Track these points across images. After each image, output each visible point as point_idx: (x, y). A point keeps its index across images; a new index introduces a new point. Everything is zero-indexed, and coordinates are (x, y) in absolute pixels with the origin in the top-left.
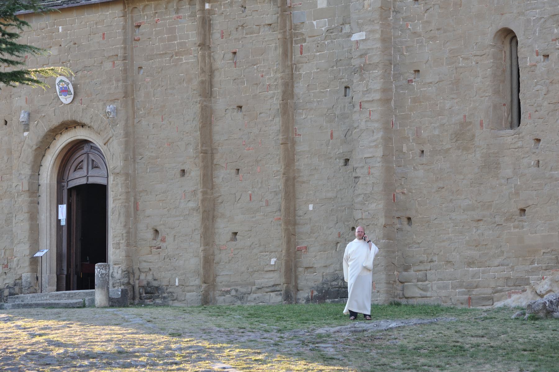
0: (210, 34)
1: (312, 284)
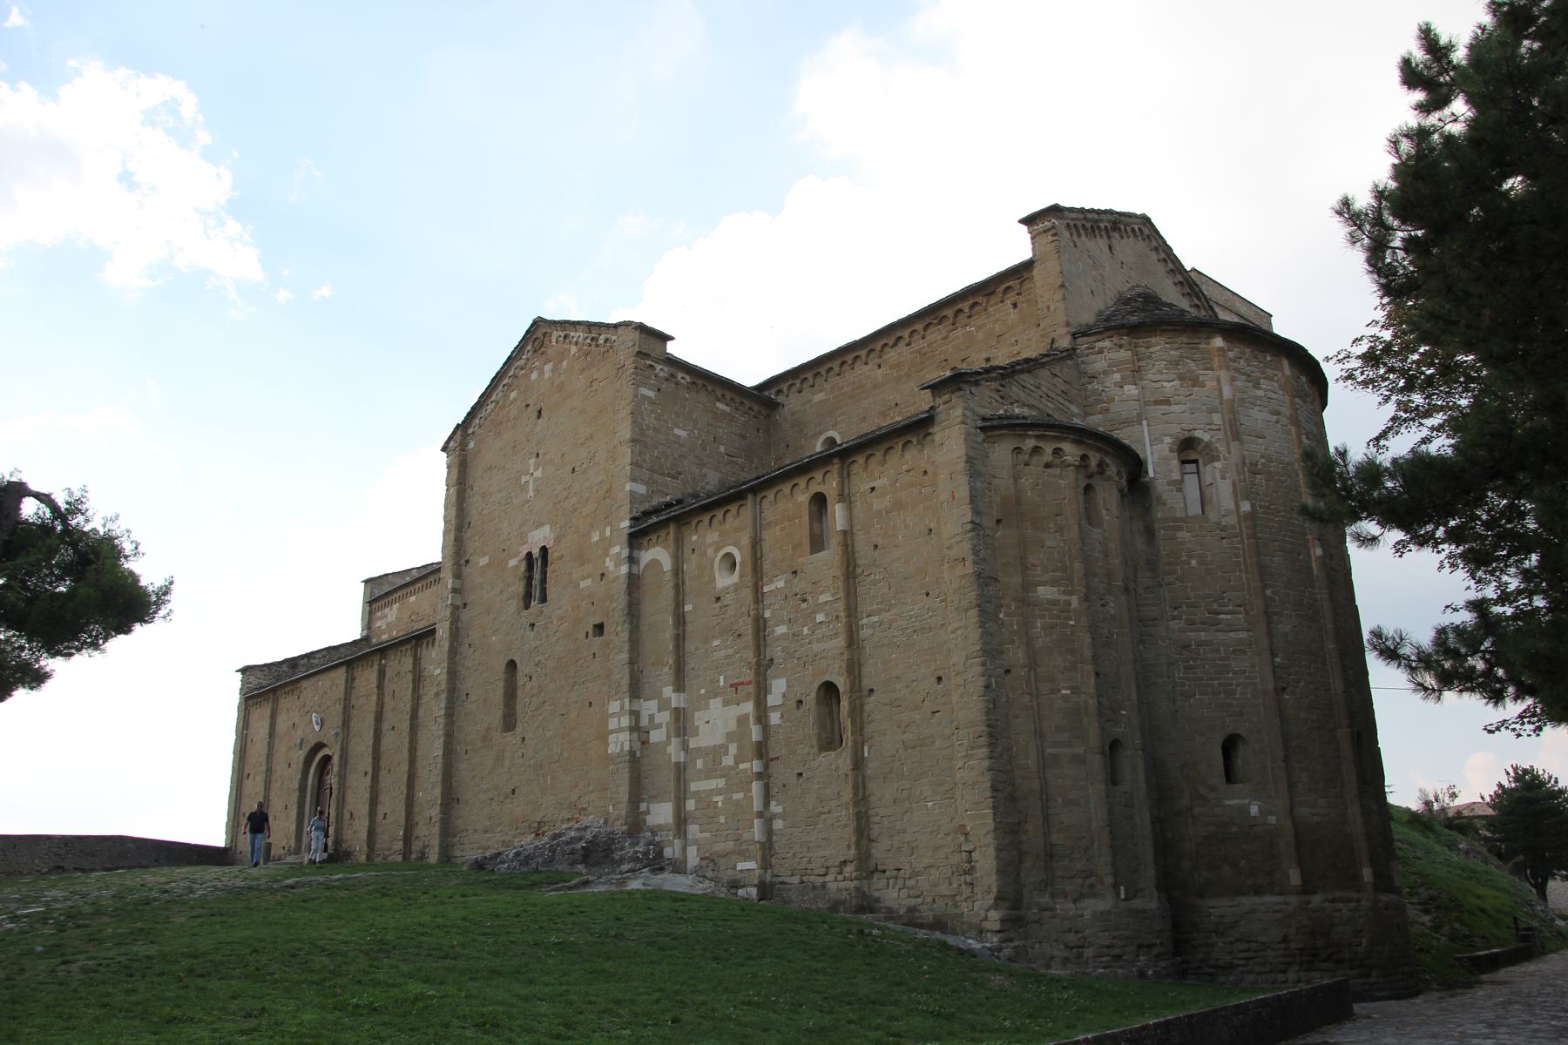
0: (384, 679)
1: (418, 848)
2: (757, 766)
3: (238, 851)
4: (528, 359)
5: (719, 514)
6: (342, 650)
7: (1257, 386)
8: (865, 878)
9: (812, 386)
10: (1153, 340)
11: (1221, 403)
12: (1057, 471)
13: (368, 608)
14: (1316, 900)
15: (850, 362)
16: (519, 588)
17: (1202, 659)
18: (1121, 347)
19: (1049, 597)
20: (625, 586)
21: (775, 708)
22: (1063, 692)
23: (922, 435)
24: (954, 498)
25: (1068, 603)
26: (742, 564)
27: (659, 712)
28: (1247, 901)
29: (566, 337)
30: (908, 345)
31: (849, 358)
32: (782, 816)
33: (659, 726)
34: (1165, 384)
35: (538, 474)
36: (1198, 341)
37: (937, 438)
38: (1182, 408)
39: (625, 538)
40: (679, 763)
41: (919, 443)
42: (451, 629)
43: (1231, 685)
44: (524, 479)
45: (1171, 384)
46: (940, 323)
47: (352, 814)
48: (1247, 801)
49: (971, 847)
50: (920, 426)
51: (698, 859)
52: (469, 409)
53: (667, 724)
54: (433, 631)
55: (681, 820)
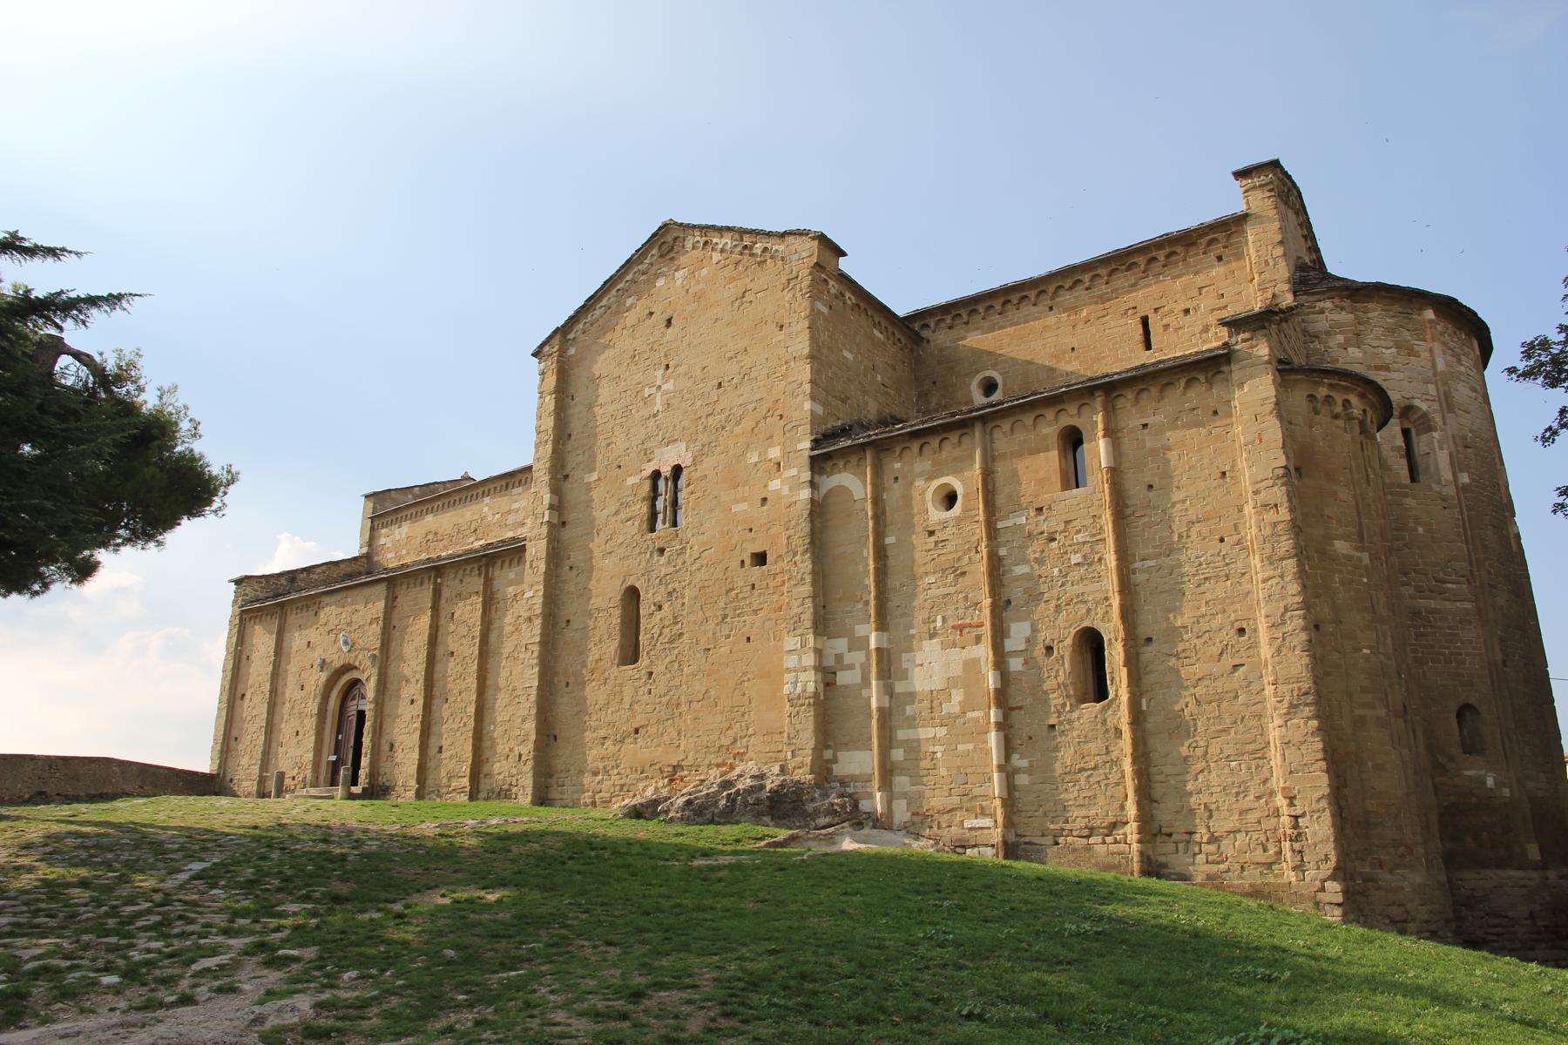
3: (228, 779)
4: (652, 264)
5: (935, 442)
6: (342, 566)
7: (1459, 361)
8: (1149, 842)
9: (967, 323)
10: (1370, 305)
11: (1435, 374)
12: (1340, 423)
13: (369, 525)
14: (1552, 875)
15: (1015, 302)
16: (643, 509)
17: (1432, 627)
18: (1342, 309)
19: (1344, 552)
20: (806, 514)
21: (1016, 653)
22: (1365, 651)
23: (1209, 375)
24: (1261, 441)
25: (1360, 559)
26: (965, 496)
27: (850, 650)
28: (1494, 876)
29: (706, 243)
30: (1087, 289)
31: (1015, 298)
32: (1029, 771)
33: (851, 667)
34: (1384, 350)
35: (669, 386)
36: (1410, 311)
37: (1236, 376)
40: (884, 708)
41: (1207, 380)
42: (548, 548)
43: (1461, 654)
44: (647, 392)
45: (1389, 351)
46: (1127, 270)
48: (1482, 772)
49: (1299, 811)
50: (1212, 366)
51: (909, 814)
52: (571, 313)
53: (861, 665)
54: (523, 549)
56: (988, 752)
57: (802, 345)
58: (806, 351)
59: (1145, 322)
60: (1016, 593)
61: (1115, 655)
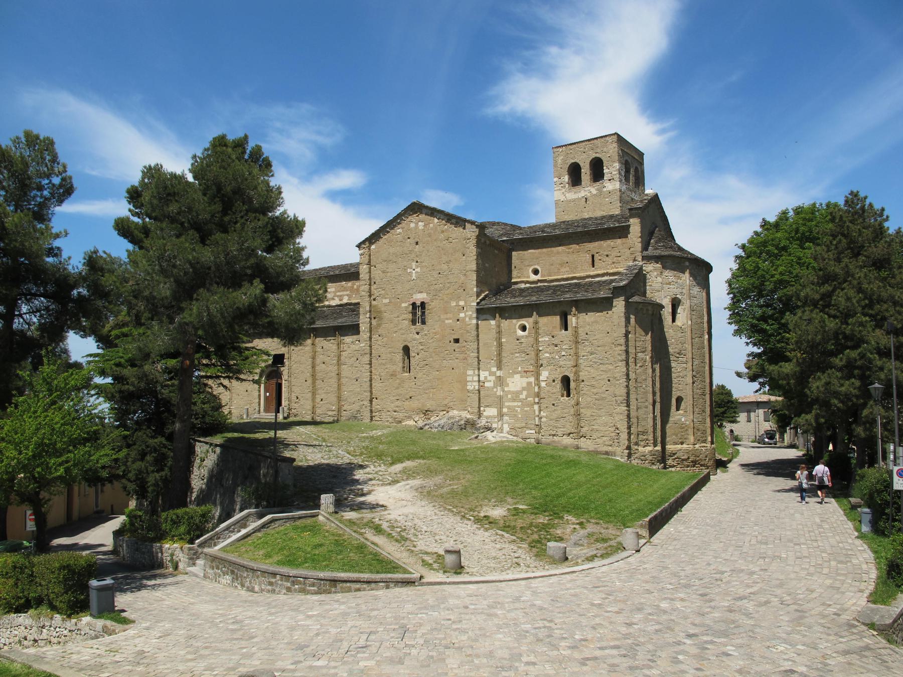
2: (537, 400)
16: (410, 316)
28: (679, 446)
35: (418, 270)
38: (673, 286)
39: (475, 310)
44: (409, 270)
47: (297, 398)
49: (618, 432)
55: (501, 415)
56: (535, 411)
57: (474, 266)
58: (475, 268)
59: (593, 256)
60: (544, 362)
61: (572, 385)
